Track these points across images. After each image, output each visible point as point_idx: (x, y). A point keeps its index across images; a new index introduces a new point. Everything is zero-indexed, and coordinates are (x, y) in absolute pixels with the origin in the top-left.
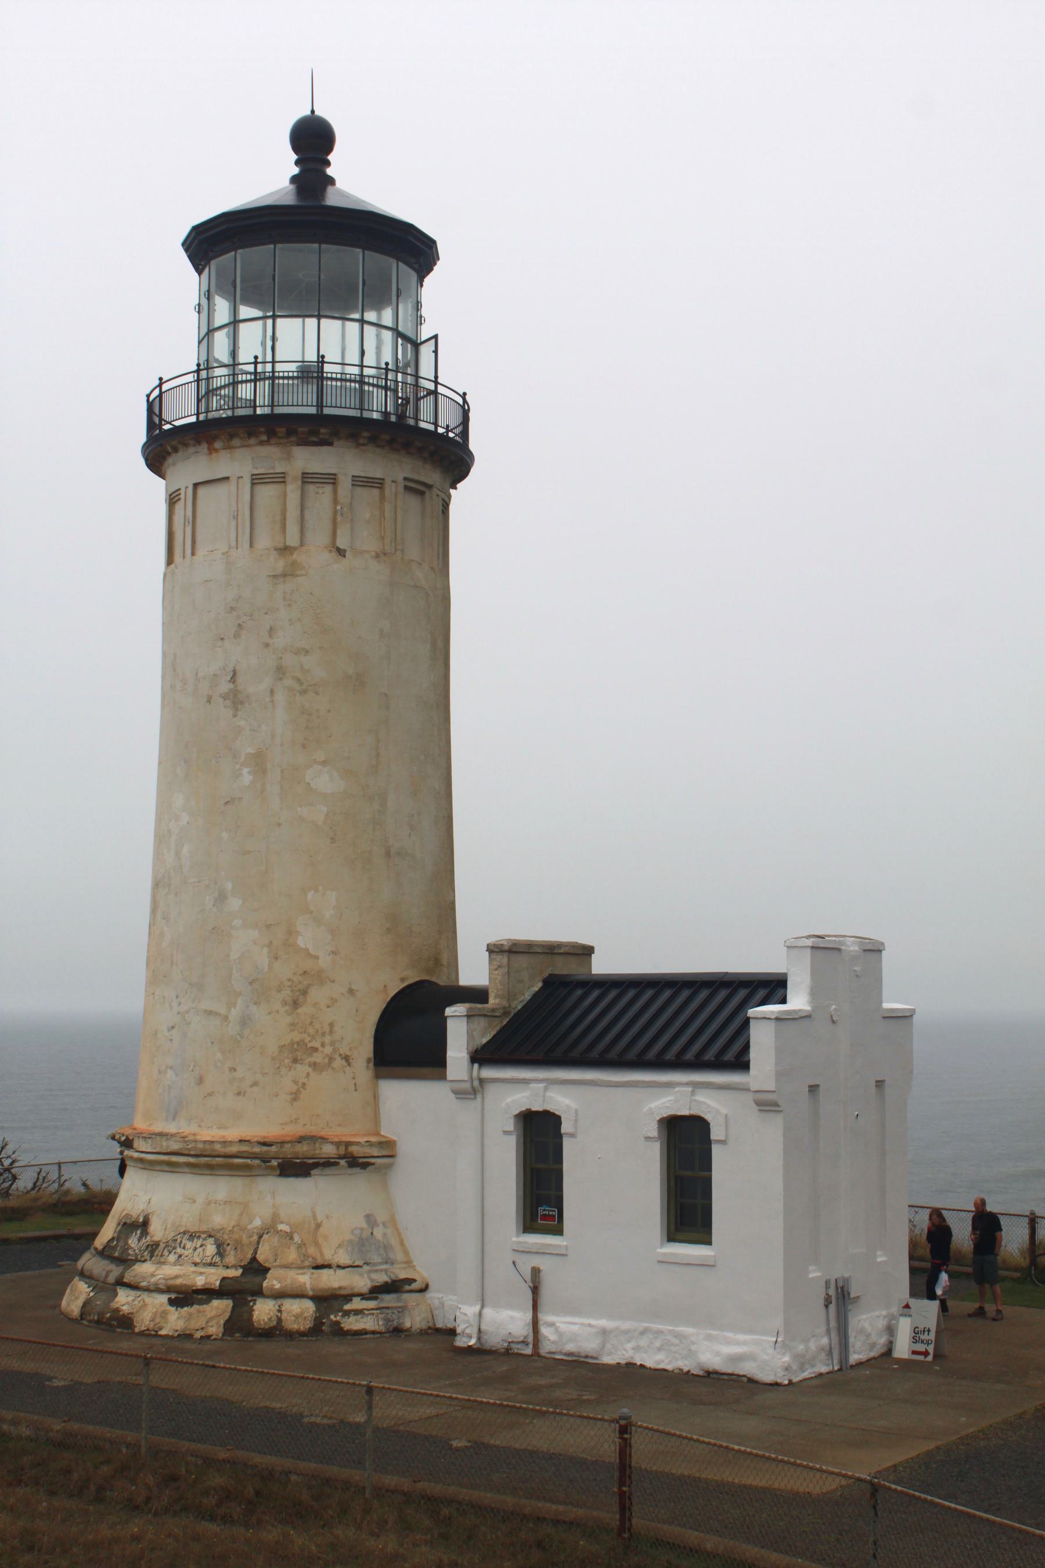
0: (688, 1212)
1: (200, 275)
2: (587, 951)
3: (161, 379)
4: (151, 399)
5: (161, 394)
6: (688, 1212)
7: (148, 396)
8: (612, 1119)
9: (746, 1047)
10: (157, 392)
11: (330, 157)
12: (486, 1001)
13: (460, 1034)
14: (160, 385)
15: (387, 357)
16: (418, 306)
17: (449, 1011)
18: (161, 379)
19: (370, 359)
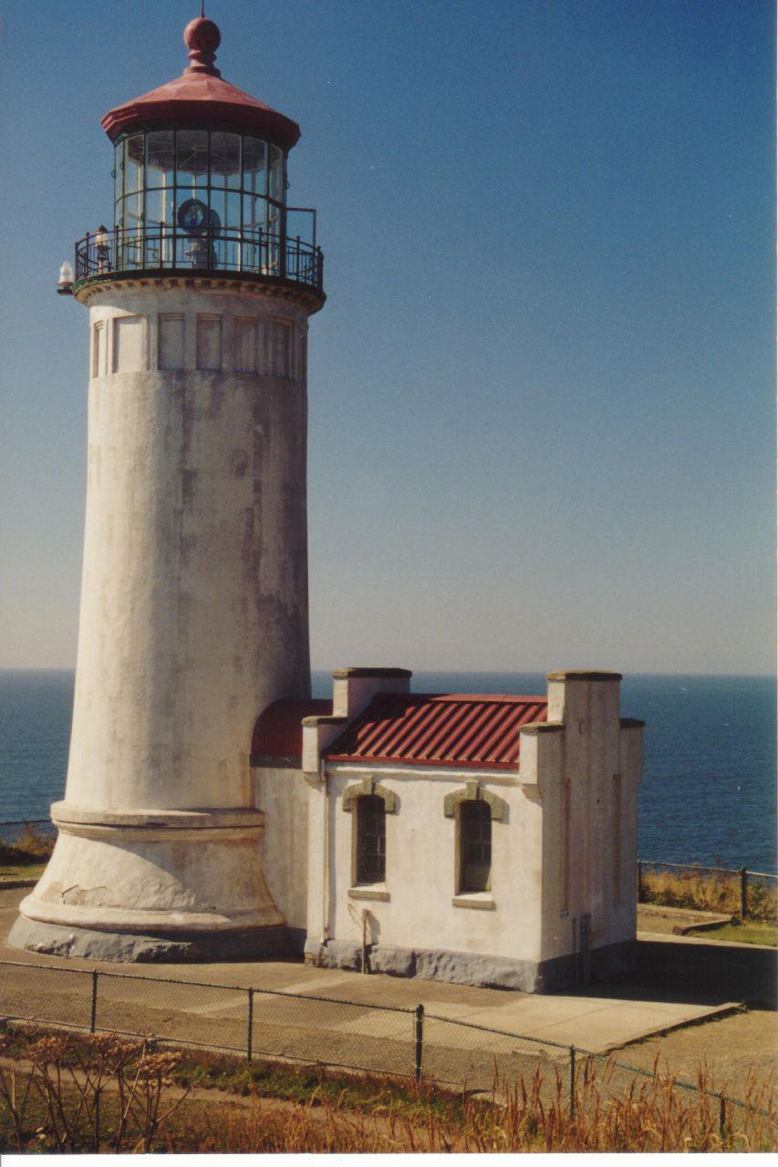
0: (473, 866)
1: (115, 146)
2: (407, 674)
3: (88, 234)
4: (79, 248)
5: (88, 246)
6: (473, 866)
7: (77, 244)
8: (422, 805)
9: (517, 754)
10: (84, 244)
11: (215, 53)
12: (331, 712)
13: (310, 738)
14: (87, 240)
15: (261, 217)
16: (285, 176)
17: (305, 720)
18: (88, 234)
19: (247, 220)
